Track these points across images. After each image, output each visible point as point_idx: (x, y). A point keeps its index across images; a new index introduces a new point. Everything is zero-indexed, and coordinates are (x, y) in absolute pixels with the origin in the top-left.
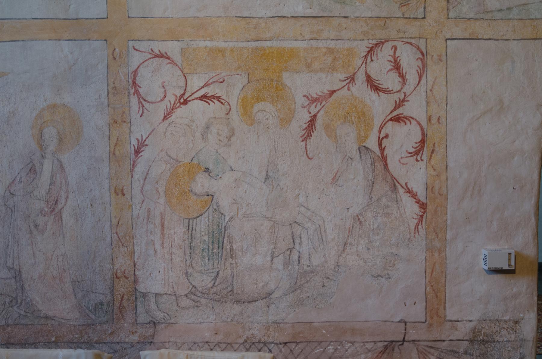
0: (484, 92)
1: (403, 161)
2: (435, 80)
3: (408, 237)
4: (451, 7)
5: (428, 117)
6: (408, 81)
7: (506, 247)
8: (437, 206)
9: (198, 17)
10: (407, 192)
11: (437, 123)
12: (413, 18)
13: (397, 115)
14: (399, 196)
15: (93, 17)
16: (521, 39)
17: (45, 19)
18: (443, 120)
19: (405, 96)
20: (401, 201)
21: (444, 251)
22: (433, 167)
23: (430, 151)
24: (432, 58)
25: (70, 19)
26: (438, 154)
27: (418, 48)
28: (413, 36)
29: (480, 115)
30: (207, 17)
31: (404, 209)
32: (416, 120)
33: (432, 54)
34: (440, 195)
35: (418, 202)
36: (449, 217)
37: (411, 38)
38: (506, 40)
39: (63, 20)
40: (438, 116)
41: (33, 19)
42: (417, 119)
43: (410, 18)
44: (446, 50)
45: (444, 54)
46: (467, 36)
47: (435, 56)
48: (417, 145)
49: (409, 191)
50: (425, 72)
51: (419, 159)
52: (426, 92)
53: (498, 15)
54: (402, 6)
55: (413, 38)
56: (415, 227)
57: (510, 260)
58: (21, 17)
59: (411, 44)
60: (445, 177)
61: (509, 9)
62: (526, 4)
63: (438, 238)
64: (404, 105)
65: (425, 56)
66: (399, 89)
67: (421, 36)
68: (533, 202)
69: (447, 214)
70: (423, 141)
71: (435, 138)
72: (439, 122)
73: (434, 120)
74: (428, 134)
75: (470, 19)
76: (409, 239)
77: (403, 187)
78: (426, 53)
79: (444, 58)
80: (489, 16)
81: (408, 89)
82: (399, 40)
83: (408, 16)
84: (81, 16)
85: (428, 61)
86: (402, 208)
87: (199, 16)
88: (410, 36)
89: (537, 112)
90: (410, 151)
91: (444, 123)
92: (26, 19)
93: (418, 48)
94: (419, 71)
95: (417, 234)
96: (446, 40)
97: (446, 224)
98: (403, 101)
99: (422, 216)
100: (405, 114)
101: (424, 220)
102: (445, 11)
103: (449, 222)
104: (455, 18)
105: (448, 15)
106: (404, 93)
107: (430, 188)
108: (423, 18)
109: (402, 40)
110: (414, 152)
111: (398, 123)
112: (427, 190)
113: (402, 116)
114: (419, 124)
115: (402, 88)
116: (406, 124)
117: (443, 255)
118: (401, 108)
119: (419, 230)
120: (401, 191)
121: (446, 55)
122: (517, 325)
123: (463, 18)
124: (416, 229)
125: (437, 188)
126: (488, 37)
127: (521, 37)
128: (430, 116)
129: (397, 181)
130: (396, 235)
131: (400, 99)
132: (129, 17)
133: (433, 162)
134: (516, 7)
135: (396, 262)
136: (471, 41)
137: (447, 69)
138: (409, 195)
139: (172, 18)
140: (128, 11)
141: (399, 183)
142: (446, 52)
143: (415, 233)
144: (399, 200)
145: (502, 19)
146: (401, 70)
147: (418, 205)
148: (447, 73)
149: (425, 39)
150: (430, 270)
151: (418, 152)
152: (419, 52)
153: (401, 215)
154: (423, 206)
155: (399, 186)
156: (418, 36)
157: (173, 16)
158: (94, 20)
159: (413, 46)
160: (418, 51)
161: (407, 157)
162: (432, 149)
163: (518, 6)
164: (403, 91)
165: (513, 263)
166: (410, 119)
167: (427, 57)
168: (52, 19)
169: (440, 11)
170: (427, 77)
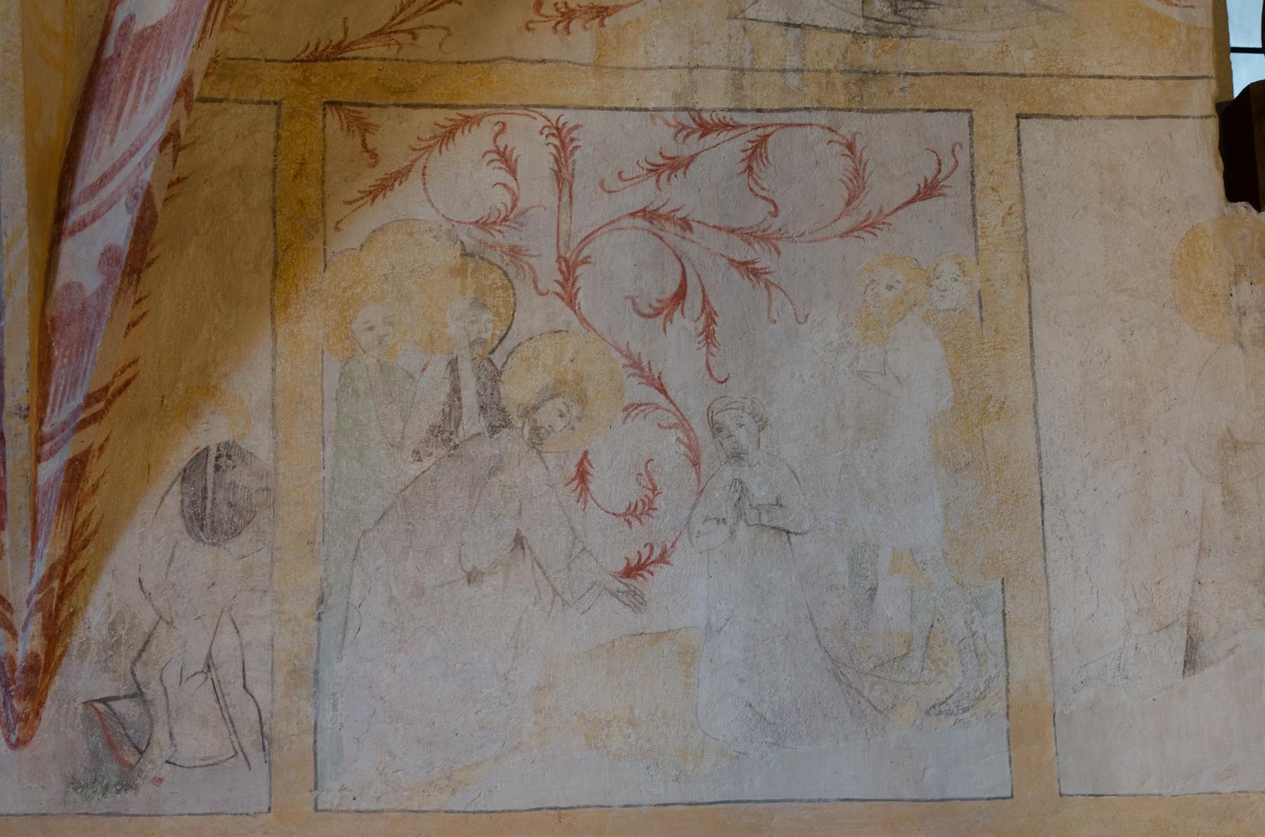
9: (1220, 793)
15: (979, 795)
17: (870, 800)
25: (927, 801)
30: (1239, 792)
39: (911, 803)
41: (842, 800)
58: (815, 796)
84: (950, 795)
87: (1223, 791)
92: (826, 801)
132: (1061, 795)
139: (1160, 795)
140: (1058, 780)
157: (1161, 792)
158: (982, 802)
168: (886, 800)
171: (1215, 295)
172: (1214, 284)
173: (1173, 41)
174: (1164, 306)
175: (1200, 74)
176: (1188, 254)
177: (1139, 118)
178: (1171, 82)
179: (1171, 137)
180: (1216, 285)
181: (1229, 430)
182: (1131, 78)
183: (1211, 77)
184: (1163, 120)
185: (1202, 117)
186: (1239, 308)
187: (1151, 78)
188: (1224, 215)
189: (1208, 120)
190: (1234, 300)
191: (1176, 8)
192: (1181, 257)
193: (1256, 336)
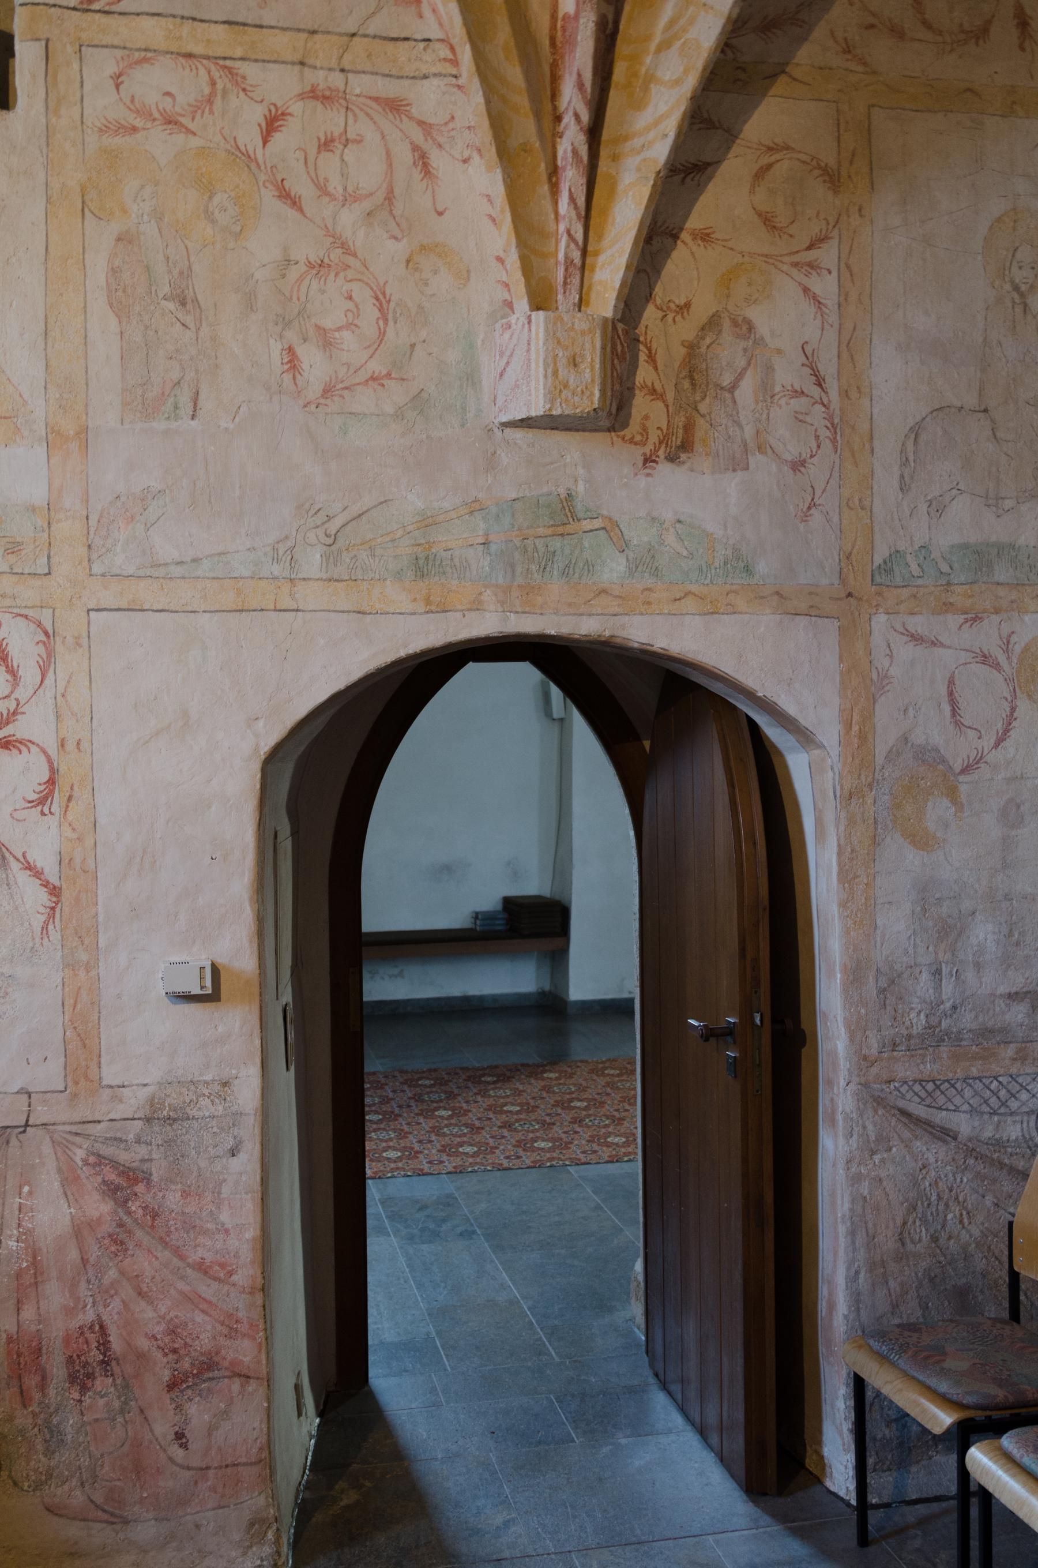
0: (155, 699)
1: (17, 815)
2: (70, 678)
3: (31, 945)
4: (94, 556)
5: (59, 741)
6: (22, 680)
7: (204, 957)
8: (80, 892)
10: (26, 868)
11: (76, 750)
12: (29, 574)
13: (5, 737)
14: (10, 876)
16: (217, 611)
18: (85, 745)
19: (18, 705)
20: (16, 884)
21: (94, 967)
22: (70, 825)
23: (66, 798)
24: (63, 642)
26: (79, 802)
27: (39, 625)
28: (29, 604)
29: (149, 737)
31: (22, 898)
32: (38, 745)
33: (64, 635)
34: (84, 871)
35: (46, 884)
36: (100, 909)
37: (25, 607)
38: (191, 612)
40: (77, 738)
42: (41, 744)
43: (22, 574)
44: (89, 627)
45: (85, 634)
46: (125, 606)
47: (68, 637)
48: (42, 788)
49: (29, 867)
50: (53, 665)
51: (46, 810)
52: (55, 698)
53: (176, 571)
54: (8, 554)
55: (28, 608)
56: (43, 928)
57: (202, 978)
59: (26, 617)
60: (93, 841)
61: (195, 560)
62: (224, 554)
63: (83, 944)
64: (17, 720)
65: (52, 638)
66: (6, 693)
67: (44, 605)
68: (246, 880)
69: (97, 904)
70: (51, 782)
71: (73, 775)
72: (79, 749)
73: (70, 746)
74: (60, 769)
75: (128, 577)
76: (32, 948)
77: (18, 860)
78: (54, 632)
79: (84, 642)
80: (161, 572)
81: (22, 693)
82: (4, 610)
83: (20, 571)
85: (57, 646)
86: (19, 896)
88: (23, 605)
89: (248, 731)
90: (31, 799)
91: (89, 751)
93: (39, 625)
94: (42, 664)
95: (46, 939)
96: (89, 611)
97: (97, 921)
98: (15, 713)
99: (53, 909)
100: (19, 736)
101: (57, 915)
102: (85, 563)
103: (101, 919)
104: (103, 575)
105: (90, 569)
106: (17, 700)
107: (67, 861)
108: (46, 574)
109: (10, 610)
110: (36, 800)
111: (7, 751)
112: (60, 864)
113: (14, 738)
114: (44, 752)
115: (12, 692)
116: (20, 753)
117: (93, 973)
118: (11, 725)
119: (50, 933)
120: (15, 866)
121: (89, 637)
122: (227, 1088)
123: (117, 575)
124: (45, 931)
125: (78, 861)
126: (160, 608)
127: (217, 607)
128: (63, 740)
129: (7, 849)
130: (9, 942)
131: (9, 710)
133: (70, 817)
134: (206, 557)
135: (10, 990)
136: (131, 613)
137: (90, 659)
138: (28, 872)
141: (11, 853)
142: (89, 632)
143: (42, 939)
144: (12, 882)
145: (184, 578)
146: (10, 661)
147: (46, 890)
148: (90, 666)
149: (51, 611)
150: (72, 1001)
151: (43, 800)
152: (41, 632)
153: (17, 908)
154: (55, 891)
155: (11, 859)
156: (39, 605)
159: (31, 621)
160: (39, 629)
161: (24, 809)
162: (68, 794)
163: (211, 556)
164: (13, 696)
165: (208, 982)
166: (29, 744)
167: (54, 640)
169: (77, 563)
170: (55, 673)
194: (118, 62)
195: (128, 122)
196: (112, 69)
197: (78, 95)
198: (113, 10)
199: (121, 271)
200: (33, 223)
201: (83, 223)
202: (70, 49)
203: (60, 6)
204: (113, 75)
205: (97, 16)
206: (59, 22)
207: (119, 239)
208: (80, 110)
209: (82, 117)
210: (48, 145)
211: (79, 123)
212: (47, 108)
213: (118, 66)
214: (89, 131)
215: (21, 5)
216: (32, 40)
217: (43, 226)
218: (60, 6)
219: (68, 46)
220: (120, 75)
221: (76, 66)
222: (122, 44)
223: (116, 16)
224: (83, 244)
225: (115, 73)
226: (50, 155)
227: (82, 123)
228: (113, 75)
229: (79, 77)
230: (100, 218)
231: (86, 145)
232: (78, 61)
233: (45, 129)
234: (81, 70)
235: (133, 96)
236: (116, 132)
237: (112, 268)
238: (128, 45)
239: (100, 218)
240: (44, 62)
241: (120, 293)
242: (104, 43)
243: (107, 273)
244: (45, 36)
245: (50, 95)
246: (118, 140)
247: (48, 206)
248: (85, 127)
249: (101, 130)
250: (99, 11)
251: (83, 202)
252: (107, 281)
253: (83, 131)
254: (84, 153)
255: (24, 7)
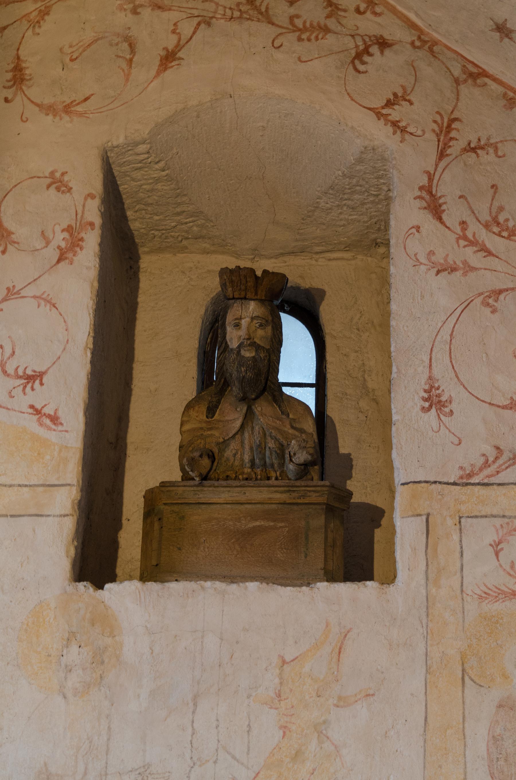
171: (49, 656)
172: (50, 646)
173: (48, 457)
174: (8, 663)
175: (64, 482)
176: (33, 623)
177: (12, 516)
178: (41, 489)
179: (34, 531)
180: (52, 648)
181: (45, 764)
182: (11, 486)
183: (73, 485)
184: (29, 518)
185: (61, 516)
186: (66, 666)
187: (26, 486)
188: (66, 592)
189: (66, 518)
190: (64, 660)
191: (54, 433)
192: (27, 625)
193: (77, 689)
194: (497, 531)
195: (509, 589)
196: (491, 537)
197: (459, 565)
198: (492, 482)
199: (503, 739)
200: (412, 694)
201: (463, 692)
202: (450, 522)
203: (440, 483)
204: (493, 543)
205: (477, 488)
206: (440, 497)
207: (500, 706)
208: (460, 579)
209: (462, 585)
210: (428, 615)
211: (459, 591)
212: (427, 579)
213: (498, 534)
214: (469, 599)
215: (403, 484)
216: (413, 516)
217: (422, 697)
218: (440, 483)
219: (448, 518)
220: (500, 543)
221: (456, 537)
222: (501, 514)
223: (495, 487)
224: (464, 713)
225: (495, 541)
226: (430, 625)
227: (462, 591)
228: (493, 543)
229: (458, 547)
230: (481, 686)
231: (466, 613)
232: (458, 531)
233: (425, 599)
234: (461, 541)
235: (513, 562)
236: (496, 599)
237: (493, 737)
238: (507, 514)
239: (481, 686)
240: (425, 535)
241: (502, 762)
242: (483, 513)
243: (488, 742)
244: (426, 512)
245: (430, 567)
246: (498, 606)
247: (428, 676)
248: (465, 595)
249: (481, 597)
250: (479, 484)
251: (463, 670)
252: (488, 750)
253: (463, 599)
254: (463, 621)
255: (406, 486)
